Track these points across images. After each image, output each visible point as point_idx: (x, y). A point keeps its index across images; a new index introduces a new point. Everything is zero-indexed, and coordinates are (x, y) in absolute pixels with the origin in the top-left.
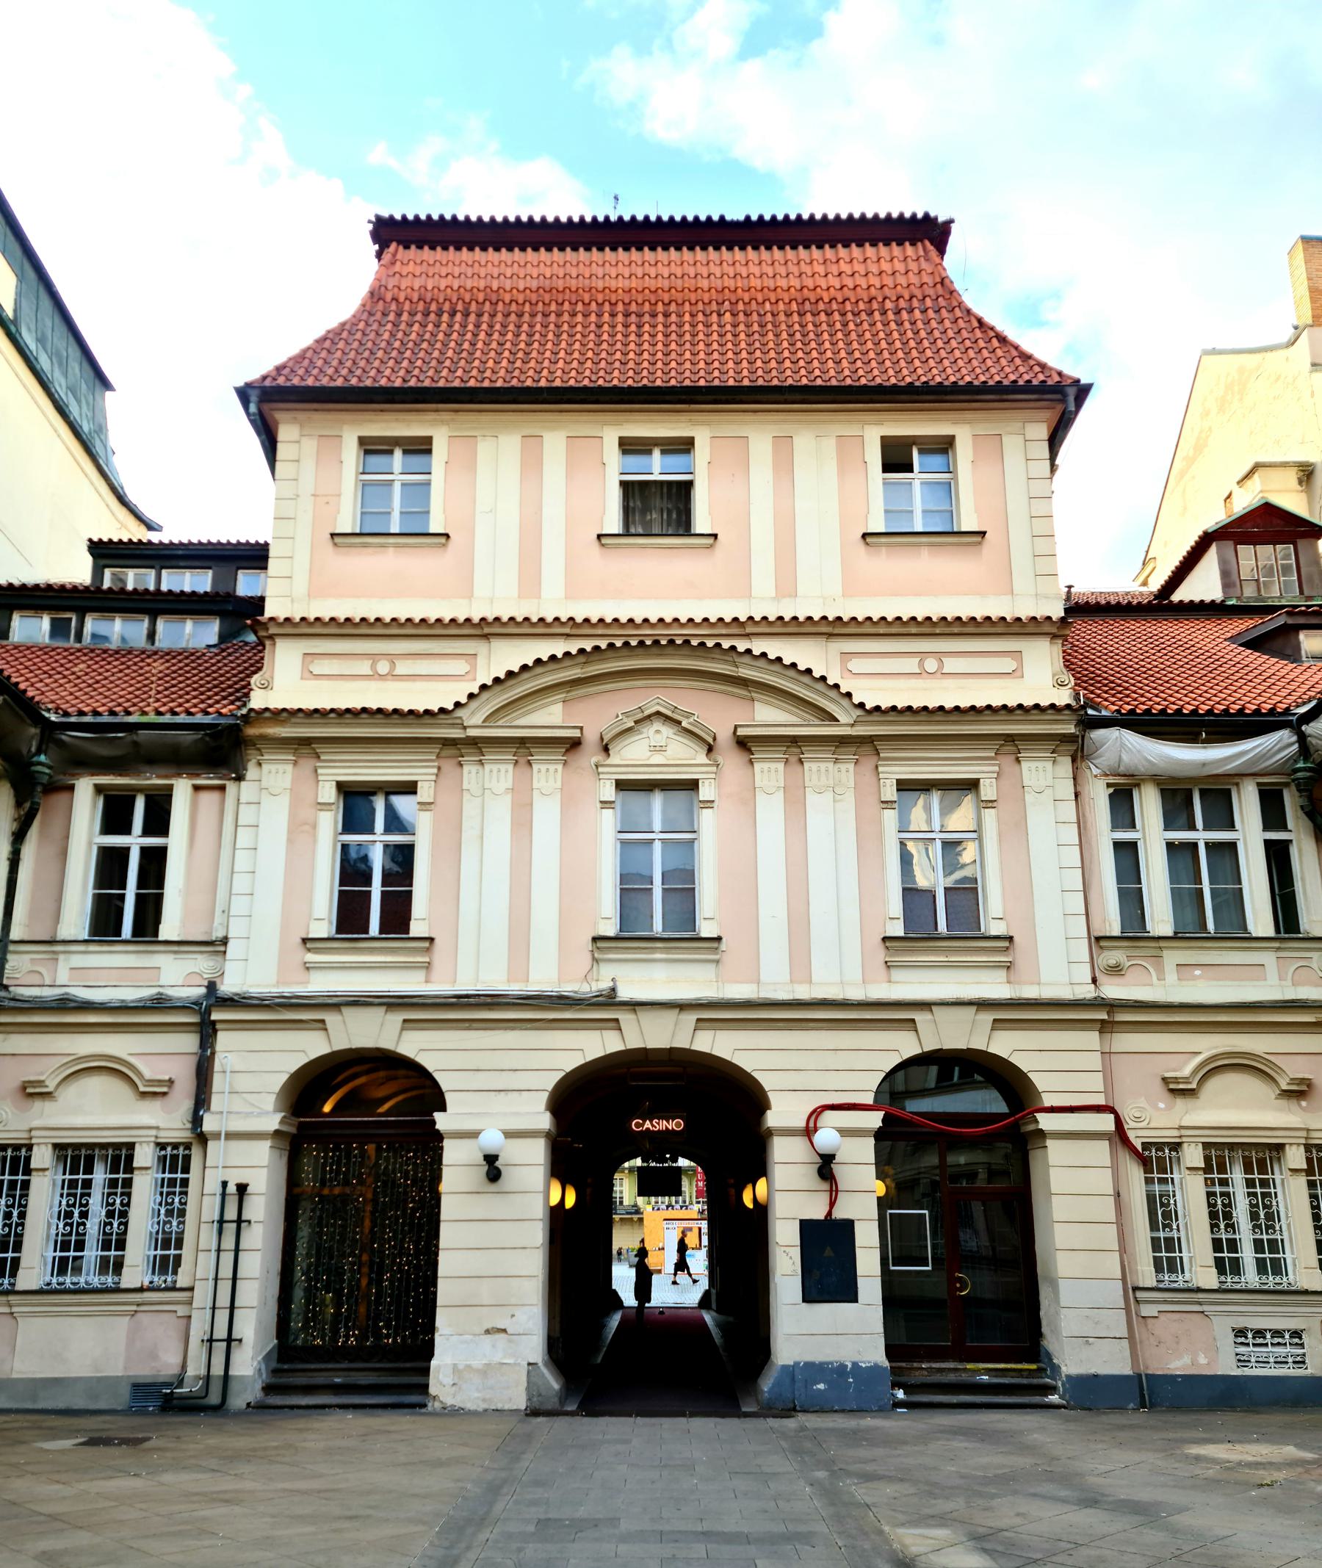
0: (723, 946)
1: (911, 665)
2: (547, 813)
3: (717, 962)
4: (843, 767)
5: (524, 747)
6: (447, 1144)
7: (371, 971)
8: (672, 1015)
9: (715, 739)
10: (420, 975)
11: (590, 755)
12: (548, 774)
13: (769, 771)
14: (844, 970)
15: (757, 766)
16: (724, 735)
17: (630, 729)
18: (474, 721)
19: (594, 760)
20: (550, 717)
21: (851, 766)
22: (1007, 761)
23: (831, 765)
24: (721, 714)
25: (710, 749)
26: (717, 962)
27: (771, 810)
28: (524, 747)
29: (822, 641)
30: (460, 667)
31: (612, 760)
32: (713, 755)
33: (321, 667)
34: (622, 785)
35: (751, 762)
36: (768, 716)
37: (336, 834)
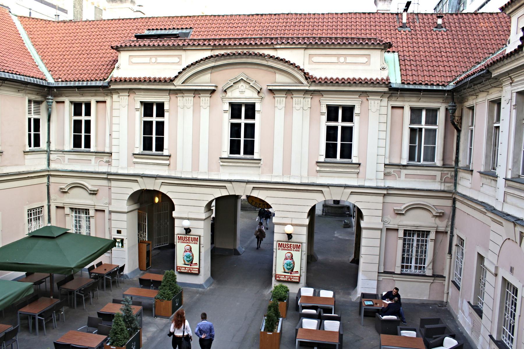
0: (262, 162)
1: (334, 59)
2: (205, 113)
3: (260, 167)
4: (307, 100)
5: (196, 92)
6: (176, 220)
7: (151, 167)
8: (244, 184)
9: (261, 89)
10: (166, 168)
11: (218, 95)
12: (205, 99)
13: (281, 100)
14: (300, 174)
15: (276, 99)
16: (265, 88)
17: (232, 86)
18: (178, 84)
19: (221, 96)
20: (205, 81)
21: (310, 99)
22: (364, 99)
23: (302, 99)
24: (265, 79)
25: (259, 92)
26: (260, 167)
27: (280, 115)
28: (196, 92)
29: (302, 51)
30: (176, 60)
31: (227, 96)
32: (260, 94)
33: (134, 60)
34: (231, 105)
35: (274, 97)
36: (281, 80)
37: (141, 118)
